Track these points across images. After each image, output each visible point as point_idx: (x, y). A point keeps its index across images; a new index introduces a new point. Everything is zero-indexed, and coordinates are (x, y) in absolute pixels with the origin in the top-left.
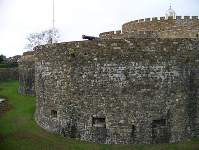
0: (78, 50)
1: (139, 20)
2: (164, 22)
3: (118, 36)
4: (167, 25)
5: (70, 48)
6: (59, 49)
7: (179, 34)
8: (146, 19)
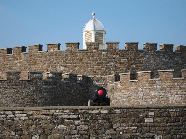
0: (149, 131)
1: (49, 45)
2: (117, 56)
4: (124, 63)
5: (124, 124)
6: (79, 124)
8: (68, 44)
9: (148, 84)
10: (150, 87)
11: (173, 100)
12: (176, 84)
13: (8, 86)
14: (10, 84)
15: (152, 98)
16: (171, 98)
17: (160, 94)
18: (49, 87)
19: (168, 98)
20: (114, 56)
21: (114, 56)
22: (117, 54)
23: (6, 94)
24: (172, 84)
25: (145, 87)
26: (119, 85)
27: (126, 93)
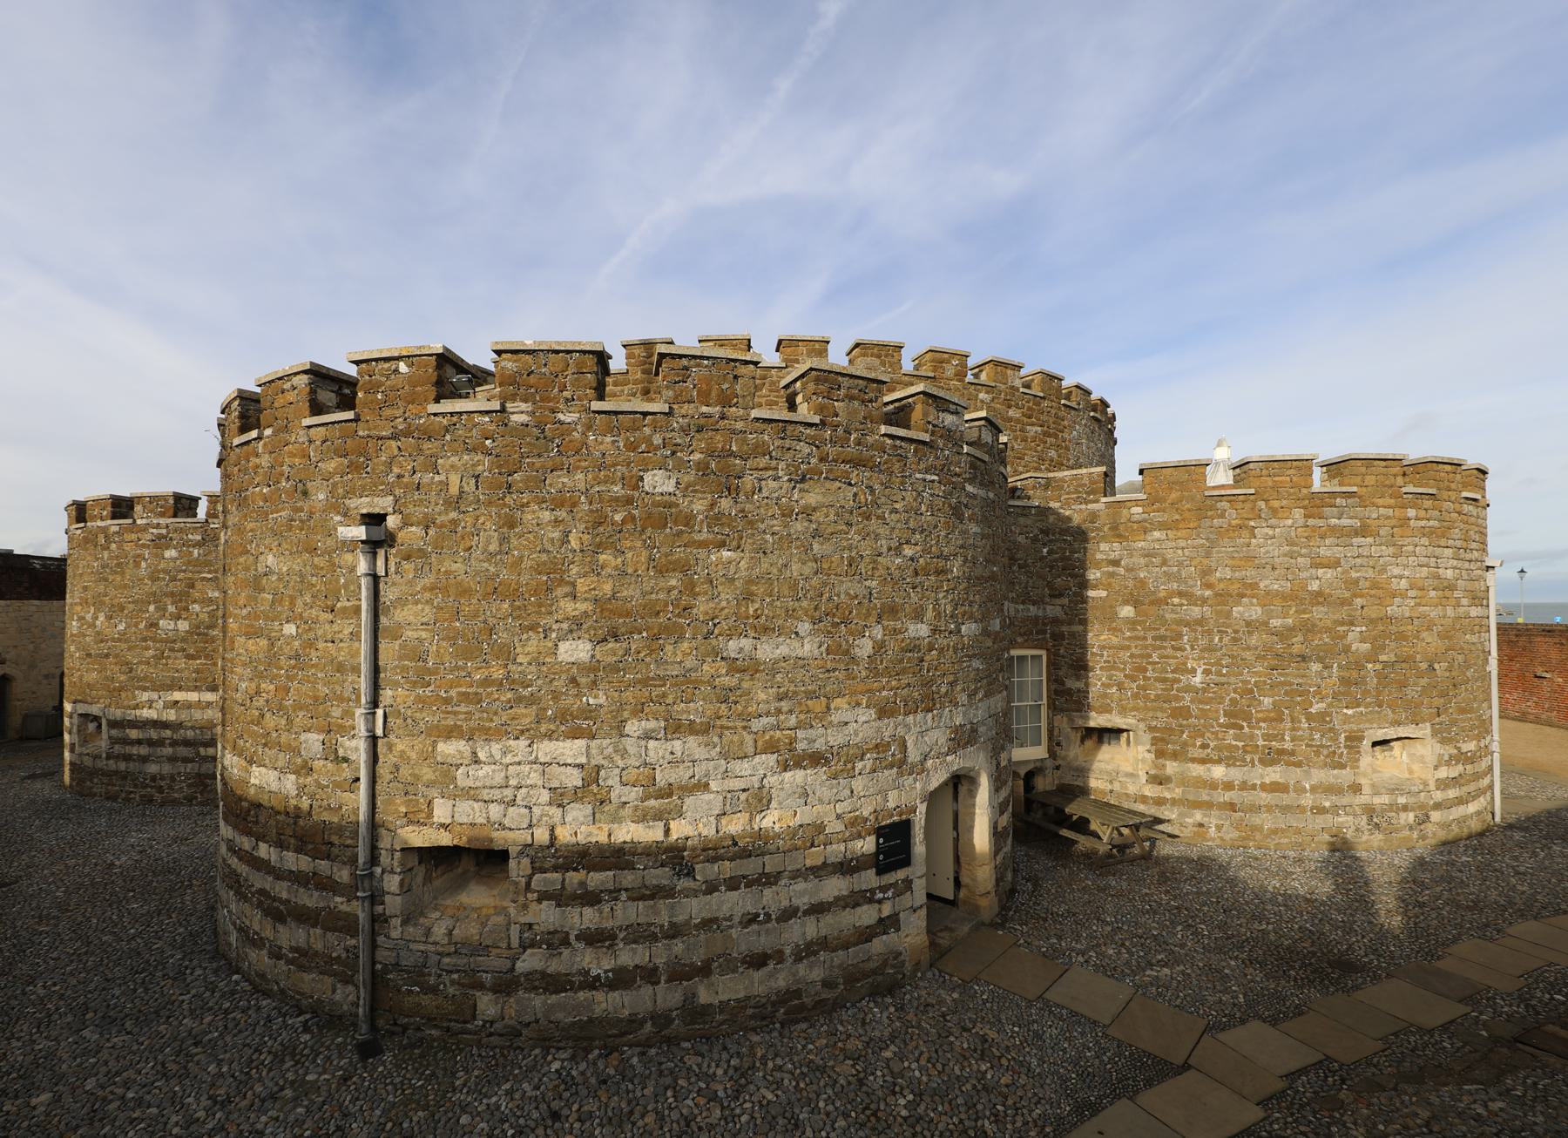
3: (857, 463)
7: (1424, 532)
9: (1304, 507)
10: (1311, 522)
11: (1401, 577)
12: (1411, 513)
13: (824, 467)
14: (832, 451)
15: (1317, 566)
16: (1396, 571)
17: (1356, 551)
18: (982, 493)
19: (1383, 570)
20: (1011, 413)
21: (1011, 413)
22: (1017, 406)
23: (808, 512)
24: (1398, 512)
25: (1290, 522)
26: (1140, 510)
27: (1182, 543)
